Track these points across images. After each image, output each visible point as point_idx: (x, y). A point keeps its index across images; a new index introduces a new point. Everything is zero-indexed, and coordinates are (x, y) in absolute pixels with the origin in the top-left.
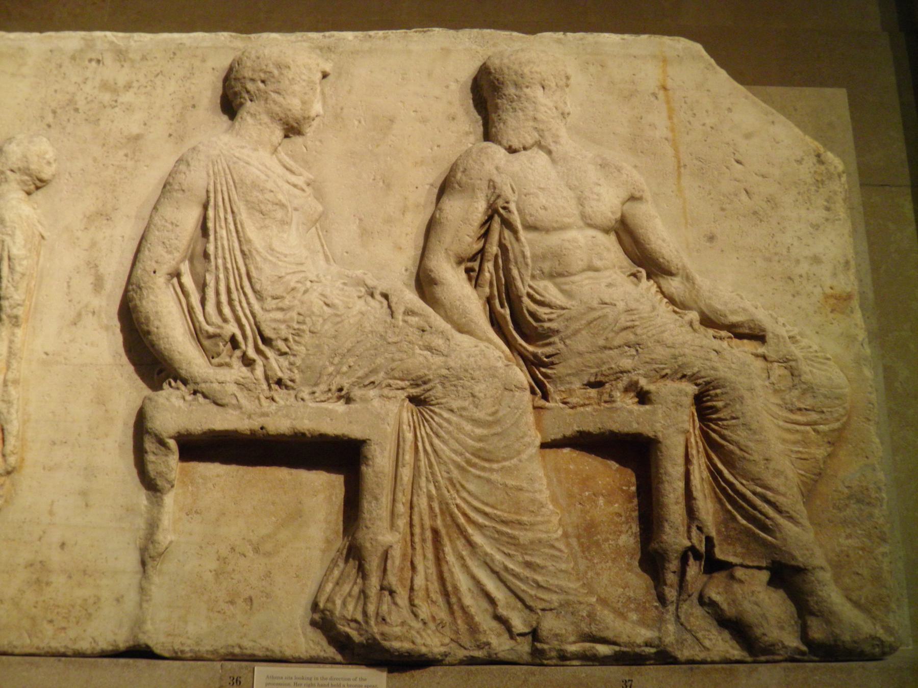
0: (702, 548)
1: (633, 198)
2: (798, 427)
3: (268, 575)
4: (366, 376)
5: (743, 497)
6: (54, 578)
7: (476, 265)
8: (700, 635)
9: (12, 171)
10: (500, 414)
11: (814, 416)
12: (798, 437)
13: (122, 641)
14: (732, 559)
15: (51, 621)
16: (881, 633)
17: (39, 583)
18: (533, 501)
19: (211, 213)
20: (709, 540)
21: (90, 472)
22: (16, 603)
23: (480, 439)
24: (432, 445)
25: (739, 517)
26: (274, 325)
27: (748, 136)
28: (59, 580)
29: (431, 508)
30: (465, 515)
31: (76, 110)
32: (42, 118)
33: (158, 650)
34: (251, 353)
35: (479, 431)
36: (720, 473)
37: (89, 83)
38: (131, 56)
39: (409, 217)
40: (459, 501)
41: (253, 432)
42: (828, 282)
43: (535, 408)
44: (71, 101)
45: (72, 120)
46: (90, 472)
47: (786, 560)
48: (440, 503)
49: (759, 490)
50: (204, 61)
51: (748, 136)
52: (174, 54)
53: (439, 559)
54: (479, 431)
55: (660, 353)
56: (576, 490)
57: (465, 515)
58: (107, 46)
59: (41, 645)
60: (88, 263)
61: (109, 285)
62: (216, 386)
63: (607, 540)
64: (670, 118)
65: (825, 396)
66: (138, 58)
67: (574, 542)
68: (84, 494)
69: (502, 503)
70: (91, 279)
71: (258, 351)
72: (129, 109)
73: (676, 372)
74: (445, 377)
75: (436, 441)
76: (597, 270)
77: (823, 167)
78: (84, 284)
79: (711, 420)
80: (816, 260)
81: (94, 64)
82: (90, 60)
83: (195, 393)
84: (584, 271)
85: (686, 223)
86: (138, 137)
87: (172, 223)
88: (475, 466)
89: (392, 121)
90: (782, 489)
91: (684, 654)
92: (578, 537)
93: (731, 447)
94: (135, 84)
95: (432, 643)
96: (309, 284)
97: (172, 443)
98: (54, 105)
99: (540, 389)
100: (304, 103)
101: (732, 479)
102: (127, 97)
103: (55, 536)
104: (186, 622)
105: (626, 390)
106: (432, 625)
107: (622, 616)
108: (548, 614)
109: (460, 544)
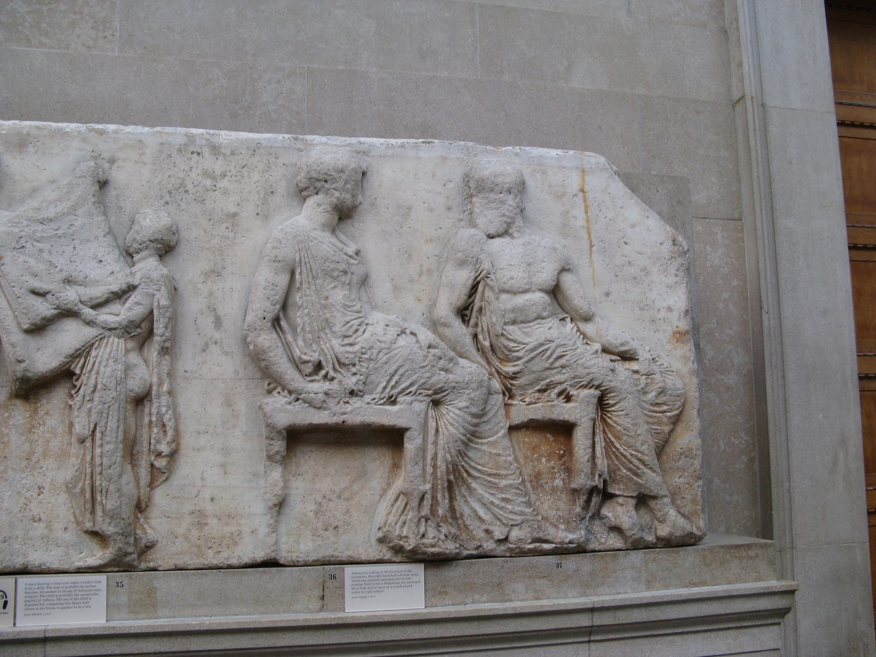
0: (601, 486)
1: (563, 270)
2: (655, 414)
3: (348, 512)
4: (408, 387)
5: (625, 456)
6: (210, 521)
7: (468, 312)
8: (598, 536)
9: (150, 241)
10: (487, 409)
11: (665, 408)
12: (656, 420)
13: (260, 555)
14: (617, 493)
15: (211, 548)
16: (695, 531)
17: (201, 525)
18: (505, 461)
19: (297, 277)
20: (605, 481)
21: (226, 451)
22: (186, 538)
23: (476, 425)
24: (448, 430)
25: (622, 468)
26: (347, 355)
27: (633, 226)
28: (213, 522)
29: (448, 467)
30: (466, 471)
31: (186, 191)
32: (162, 197)
33: (282, 562)
34: (332, 373)
35: (475, 421)
36: (612, 443)
37: (194, 170)
38: (223, 151)
39: (424, 278)
40: (463, 463)
41: (337, 424)
42: (676, 324)
43: (506, 405)
44: (182, 185)
46: (226, 451)
47: (647, 492)
48: (453, 465)
49: (634, 452)
50: (277, 158)
51: (633, 226)
52: (254, 151)
53: (452, 499)
54: (475, 421)
55: (581, 371)
56: (529, 454)
57: (466, 471)
58: (204, 142)
59: (206, 563)
60: (209, 308)
61: (226, 324)
62: (312, 395)
63: (547, 483)
64: (586, 212)
65: (671, 395)
66: (228, 153)
67: (528, 484)
68: (223, 465)
69: (488, 464)
70: (212, 319)
71: (335, 369)
72: (226, 192)
73: (589, 383)
74: (454, 388)
75: (451, 428)
76: (544, 318)
77: (676, 248)
78: (207, 323)
79: (608, 411)
80: (670, 309)
82: (192, 153)
83: (298, 400)
84: (536, 319)
85: (595, 285)
86: (234, 215)
87: (273, 284)
88: (471, 441)
89: (410, 208)
90: (646, 452)
91: (591, 546)
92: (531, 481)
93: (619, 428)
94: (228, 173)
95: (450, 547)
96: (365, 327)
97: (285, 433)
98: (170, 187)
99: (508, 393)
100: (353, 196)
101: (618, 445)
102: (224, 183)
103: (207, 494)
104: (299, 544)
105: (559, 394)
106: (450, 537)
107: (557, 527)
108: (516, 528)
109: (463, 489)
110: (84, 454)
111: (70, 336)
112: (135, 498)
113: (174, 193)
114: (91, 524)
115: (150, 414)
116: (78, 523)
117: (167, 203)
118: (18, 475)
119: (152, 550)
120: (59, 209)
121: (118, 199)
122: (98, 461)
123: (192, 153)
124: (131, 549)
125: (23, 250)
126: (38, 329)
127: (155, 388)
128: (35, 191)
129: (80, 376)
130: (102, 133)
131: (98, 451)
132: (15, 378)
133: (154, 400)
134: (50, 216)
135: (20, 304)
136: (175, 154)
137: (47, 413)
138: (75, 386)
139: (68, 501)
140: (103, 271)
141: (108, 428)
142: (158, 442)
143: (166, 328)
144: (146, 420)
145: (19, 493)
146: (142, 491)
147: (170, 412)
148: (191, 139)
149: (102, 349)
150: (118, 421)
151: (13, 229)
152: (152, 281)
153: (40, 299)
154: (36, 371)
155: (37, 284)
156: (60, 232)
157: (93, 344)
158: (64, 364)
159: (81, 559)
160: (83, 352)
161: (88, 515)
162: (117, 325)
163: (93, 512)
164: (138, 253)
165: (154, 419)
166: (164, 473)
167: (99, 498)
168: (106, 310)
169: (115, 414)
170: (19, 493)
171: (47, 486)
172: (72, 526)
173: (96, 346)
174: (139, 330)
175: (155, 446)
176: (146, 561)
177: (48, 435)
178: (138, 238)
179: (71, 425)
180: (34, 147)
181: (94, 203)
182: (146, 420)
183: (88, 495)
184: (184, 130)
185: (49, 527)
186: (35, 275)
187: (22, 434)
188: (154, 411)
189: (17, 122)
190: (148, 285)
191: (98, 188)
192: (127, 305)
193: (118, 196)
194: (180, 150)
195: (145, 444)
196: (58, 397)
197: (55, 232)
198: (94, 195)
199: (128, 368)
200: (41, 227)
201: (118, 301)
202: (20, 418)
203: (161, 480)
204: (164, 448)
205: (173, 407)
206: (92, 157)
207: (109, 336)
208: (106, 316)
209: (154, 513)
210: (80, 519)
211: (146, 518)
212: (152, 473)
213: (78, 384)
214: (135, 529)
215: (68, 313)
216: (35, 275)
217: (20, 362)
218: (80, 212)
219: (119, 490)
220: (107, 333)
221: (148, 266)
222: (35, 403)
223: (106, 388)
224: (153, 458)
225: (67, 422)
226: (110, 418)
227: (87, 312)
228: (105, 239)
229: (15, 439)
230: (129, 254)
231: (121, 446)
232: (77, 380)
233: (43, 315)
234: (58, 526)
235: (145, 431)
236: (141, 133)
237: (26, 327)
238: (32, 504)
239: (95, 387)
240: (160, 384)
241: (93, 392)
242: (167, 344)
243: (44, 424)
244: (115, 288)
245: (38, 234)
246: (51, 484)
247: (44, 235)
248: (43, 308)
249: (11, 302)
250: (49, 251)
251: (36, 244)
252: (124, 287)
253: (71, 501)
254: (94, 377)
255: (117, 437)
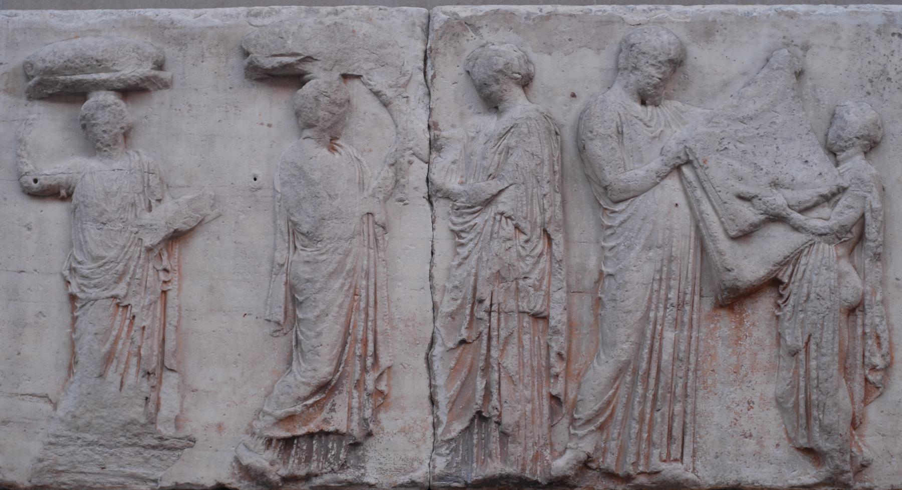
9: (858, 138)
31: (889, 79)
32: (863, 87)
37: (896, 54)
44: (884, 72)
45: (887, 89)
81: (896, 37)
82: (893, 34)
98: (870, 75)
110: (797, 368)
111: (778, 243)
112: (851, 414)
113: (876, 82)
114: (805, 440)
115: (864, 325)
116: (790, 440)
117: (869, 93)
118: (727, 389)
119: (867, 470)
120: (758, 106)
121: (814, 90)
122: (814, 374)
123: (893, 34)
124: (847, 467)
125: (726, 151)
126: (744, 236)
127: (868, 297)
128: (726, 84)
129: (788, 284)
130: (792, 16)
131: (813, 363)
132: (723, 288)
133: (868, 310)
134: (750, 114)
135: (727, 209)
136: (874, 36)
137: (753, 324)
138: (781, 296)
139: (779, 416)
140: (810, 173)
141: (824, 340)
142: (873, 354)
143: (878, 232)
144: (859, 331)
145: (728, 407)
146: (856, 406)
147: (884, 323)
148: (890, 19)
149: (813, 256)
150: (834, 332)
151: (714, 129)
152: (862, 182)
153: (746, 204)
154: (745, 280)
155: (743, 189)
156: (761, 131)
157: (802, 251)
158: (772, 272)
159: (794, 477)
160: (792, 259)
161: (802, 431)
162: (828, 230)
163: (808, 427)
164: (843, 151)
165: (868, 330)
166: (878, 388)
167: (815, 413)
168: (814, 214)
169: (830, 325)
170: (728, 407)
171: (756, 400)
172: (784, 443)
173: (805, 252)
174: (849, 235)
175: (869, 358)
176: (861, 481)
177: (755, 347)
178: (843, 135)
179: (779, 336)
180: (721, 35)
181: (793, 98)
182: (859, 331)
183: (802, 410)
184: (880, 8)
185: (760, 443)
186: (741, 179)
187: (729, 347)
188: (867, 321)
189: (700, 7)
190: (859, 187)
191: (795, 80)
192: (837, 209)
193: (814, 87)
194: (879, 32)
195: (859, 356)
196: (764, 306)
197: (757, 132)
198: (793, 89)
199: (841, 276)
200: (741, 126)
201: (826, 204)
202: (726, 329)
203: (875, 395)
204: (878, 361)
205: (886, 317)
206: (784, 44)
207: (819, 242)
208: (816, 221)
209: (868, 430)
210: (793, 435)
211: (861, 436)
212: (866, 387)
213: (785, 293)
214: (851, 446)
215: (775, 218)
216: (741, 179)
217: (729, 271)
218: (778, 109)
219: (836, 404)
220: (817, 239)
221: (855, 164)
222: (741, 314)
223: (819, 297)
224: (867, 372)
225: (774, 334)
226: (825, 329)
227: (796, 216)
228: (808, 137)
229: (722, 351)
230: (833, 152)
231: (836, 358)
232: (784, 288)
233: (751, 221)
234: (770, 443)
235: (859, 342)
236: (835, 15)
237: (733, 234)
238: (742, 419)
239: (808, 296)
240: (874, 293)
241: (806, 301)
242: (879, 250)
243: (751, 335)
244: (825, 190)
245: (740, 135)
246: (761, 399)
247: (745, 134)
248: (749, 214)
249: (717, 207)
250: (753, 152)
251: (738, 145)
252: (834, 189)
253: (783, 417)
254: (806, 285)
255: (832, 349)
